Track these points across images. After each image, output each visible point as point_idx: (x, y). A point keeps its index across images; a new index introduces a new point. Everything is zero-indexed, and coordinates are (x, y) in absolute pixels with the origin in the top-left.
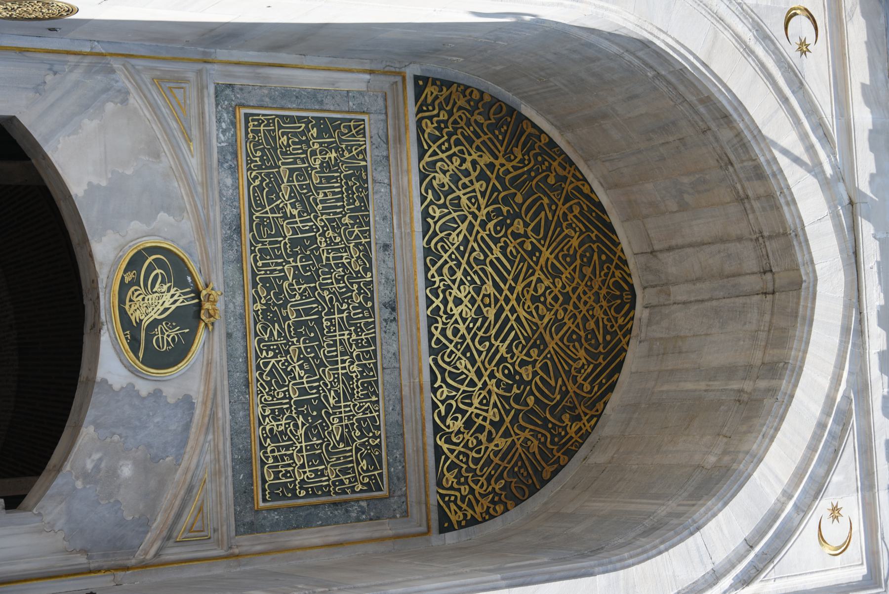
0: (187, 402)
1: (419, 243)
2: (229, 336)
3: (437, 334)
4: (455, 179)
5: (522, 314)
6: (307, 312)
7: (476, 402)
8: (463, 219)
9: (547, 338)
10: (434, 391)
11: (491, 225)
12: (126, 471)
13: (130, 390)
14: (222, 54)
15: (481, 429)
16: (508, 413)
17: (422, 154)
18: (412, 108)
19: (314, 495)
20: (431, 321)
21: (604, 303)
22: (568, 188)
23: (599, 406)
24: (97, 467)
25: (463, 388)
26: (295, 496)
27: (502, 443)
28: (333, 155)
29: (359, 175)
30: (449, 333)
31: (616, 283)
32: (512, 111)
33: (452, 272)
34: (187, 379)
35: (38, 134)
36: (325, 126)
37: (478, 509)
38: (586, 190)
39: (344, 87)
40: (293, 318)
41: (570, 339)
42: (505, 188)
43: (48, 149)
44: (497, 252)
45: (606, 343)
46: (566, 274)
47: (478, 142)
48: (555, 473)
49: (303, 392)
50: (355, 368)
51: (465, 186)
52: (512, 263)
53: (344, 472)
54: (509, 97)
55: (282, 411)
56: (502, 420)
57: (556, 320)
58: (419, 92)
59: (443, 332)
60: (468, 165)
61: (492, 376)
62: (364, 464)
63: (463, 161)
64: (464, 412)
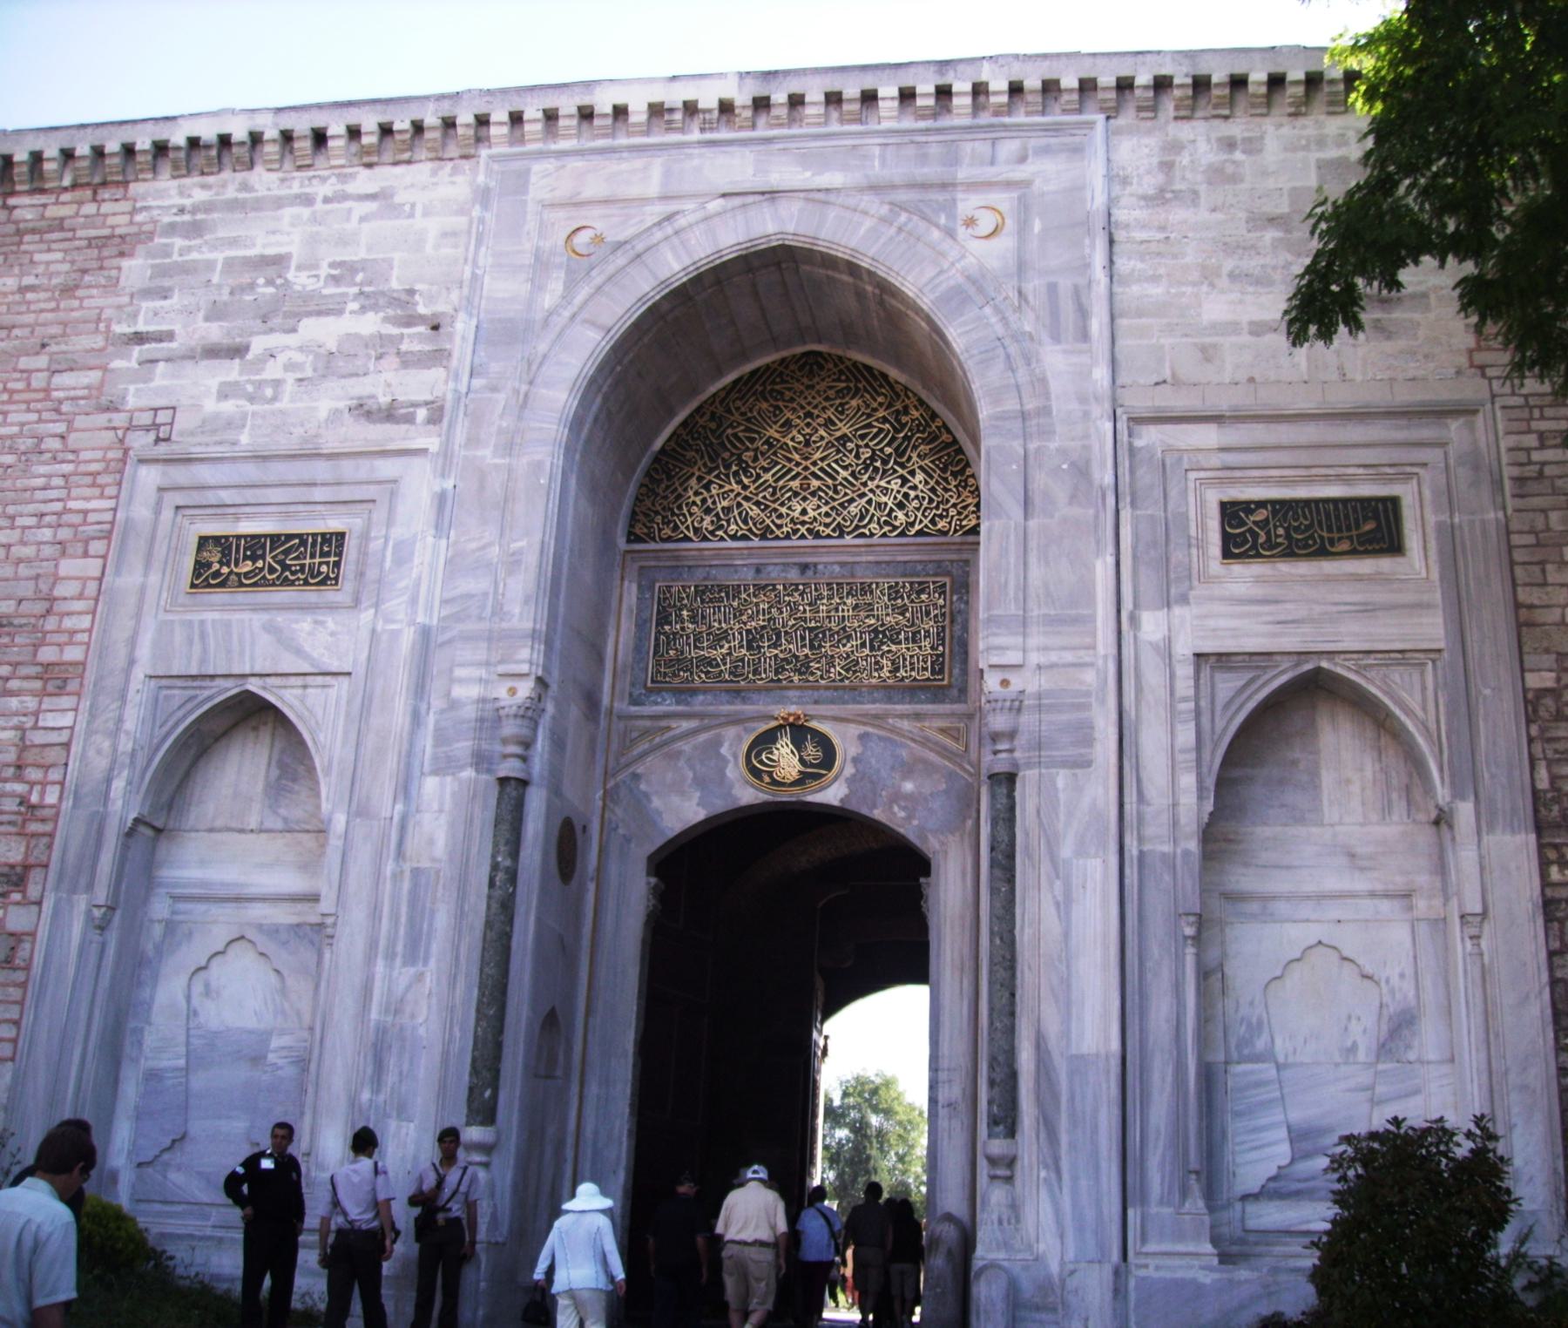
0: (863, 738)
1: (756, 542)
2: (816, 702)
3: (828, 531)
4: (708, 511)
5: (818, 455)
6: (803, 638)
7: (884, 499)
8: (739, 505)
9: (838, 434)
10: (872, 535)
11: (746, 481)
12: (908, 786)
13: (851, 781)
14: (606, 700)
15: (906, 495)
16: (895, 471)
17: (687, 539)
18: (652, 546)
19: (943, 639)
20: (817, 535)
21: (816, 379)
22: (720, 411)
23: (898, 388)
24: (904, 808)
25: (872, 510)
26: (943, 655)
27: (920, 476)
28: (685, 613)
30: (828, 520)
31: (801, 369)
32: (656, 460)
33: (780, 516)
34: (845, 740)
35: (659, 842)
36: (663, 619)
37: (970, 500)
38: (723, 394)
39: (634, 599)
40: (807, 651)
41: (842, 413)
42: (717, 467)
43: (671, 835)
44: (768, 476)
45: (848, 380)
46: (788, 415)
47: (680, 490)
48: (949, 431)
49: (863, 645)
50: (849, 601)
51: (714, 503)
52: (777, 463)
53: (928, 613)
54: (645, 462)
55: (877, 663)
56: (902, 477)
57: (825, 425)
58: (639, 540)
59: (827, 525)
60: (698, 500)
62: (924, 597)
63: (694, 503)
64: (892, 510)
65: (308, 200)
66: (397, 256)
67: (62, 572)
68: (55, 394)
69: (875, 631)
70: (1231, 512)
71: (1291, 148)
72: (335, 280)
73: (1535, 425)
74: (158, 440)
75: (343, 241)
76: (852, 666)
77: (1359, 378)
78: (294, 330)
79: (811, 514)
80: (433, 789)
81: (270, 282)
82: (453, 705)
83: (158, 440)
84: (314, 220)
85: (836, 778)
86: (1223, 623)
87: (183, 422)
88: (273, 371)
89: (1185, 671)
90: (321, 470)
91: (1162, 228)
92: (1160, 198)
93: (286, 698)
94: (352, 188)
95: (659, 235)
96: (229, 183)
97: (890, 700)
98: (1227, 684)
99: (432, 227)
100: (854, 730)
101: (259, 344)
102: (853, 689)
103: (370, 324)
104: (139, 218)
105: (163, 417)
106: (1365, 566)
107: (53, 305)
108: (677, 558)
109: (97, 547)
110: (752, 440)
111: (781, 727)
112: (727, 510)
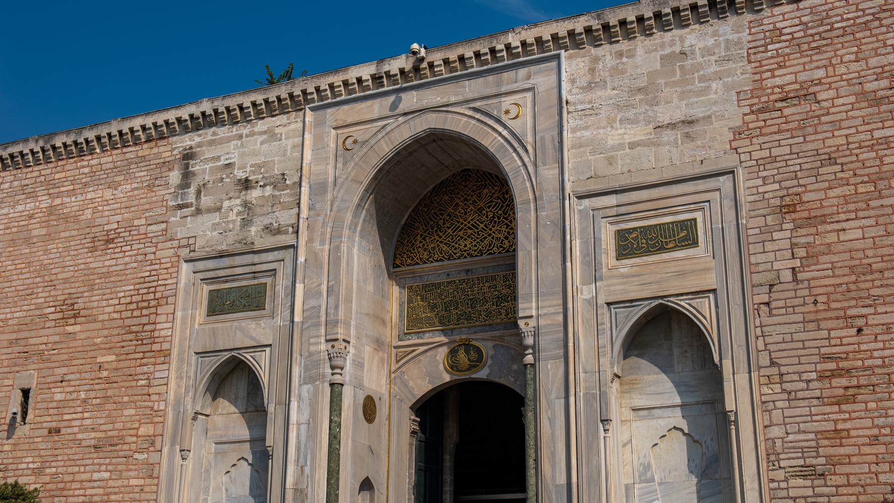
4: (425, 250)
15: (508, 233)
17: (417, 264)
18: (403, 268)
20: (472, 256)
24: (513, 377)
32: (403, 228)
33: (456, 249)
34: (487, 348)
44: (449, 231)
49: (493, 304)
56: (506, 224)
58: (398, 266)
60: (421, 245)
61: (491, 230)
66: (276, 159)
67: (159, 312)
68: (149, 235)
69: (498, 297)
70: (621, 235)
71: (649, 52)
72: (254, 172)
73: (760, 174)
74: (191, 251)
75: (255, 154)
76: (489, 314)
77: (678, 163)
78: (239, 197)
79: (469, 246)
81: (228, 177)
82: (311, 354)
83: (191, 251)
85: (484, 366)
86: (618, 287)
87: (200, 243)
88: (232, 216)
90: (256, 258)
91: (590, 102)
92: (589, 87)
94: (256, 129)
95: (380, 136)
96: (208, 134)
97: (506, 329)
99: (290, 143)
100: (490, 344)
101: (226, 204)
102: (490, 325)
104: (174, 153)
105: (192, 241)
107: (144, 196)
108: (413, 273)
109: (170, 300)
110: (442, 215)
111: (460, 345)
112: (434, 248)
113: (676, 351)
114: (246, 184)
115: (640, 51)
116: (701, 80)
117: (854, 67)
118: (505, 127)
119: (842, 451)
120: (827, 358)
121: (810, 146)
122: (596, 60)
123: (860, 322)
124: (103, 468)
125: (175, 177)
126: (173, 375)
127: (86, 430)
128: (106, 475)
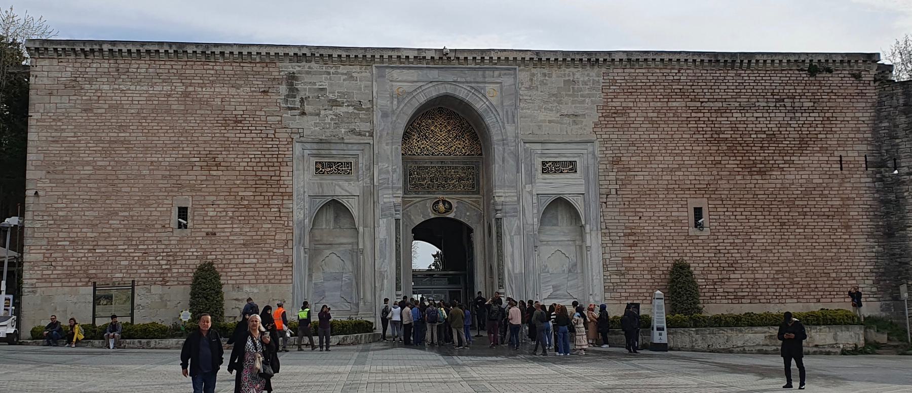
29: (419, 168)
34: (454, 205)
36: (411, 175)
65: (329, 73)
70: (544, 163)
80: (383, 222)
84: (330, 79)
87: (306, 132)
88: (328, 120)
89: (535, 197)
92: (529, 88)
93: (345, 202)
96: (305, 66)
98: (543, 199)
101: (322, 112)
103: (351, 109)
105: (300, 131)
106: (568, 176)
113: (560, 217)
114: (334, 103)
115: (554, 75)
116: (582, 96)
117: (645, 105)
118: (488, 100)
119: (631, 265)
120: (626, 228)
121: (626, 137)
122: (533, 75)
123: (641, 214)
124: (252, 256)
125: (283, 89)
126: (295, 207)
127: (235, 235)
128: (255, 261)
